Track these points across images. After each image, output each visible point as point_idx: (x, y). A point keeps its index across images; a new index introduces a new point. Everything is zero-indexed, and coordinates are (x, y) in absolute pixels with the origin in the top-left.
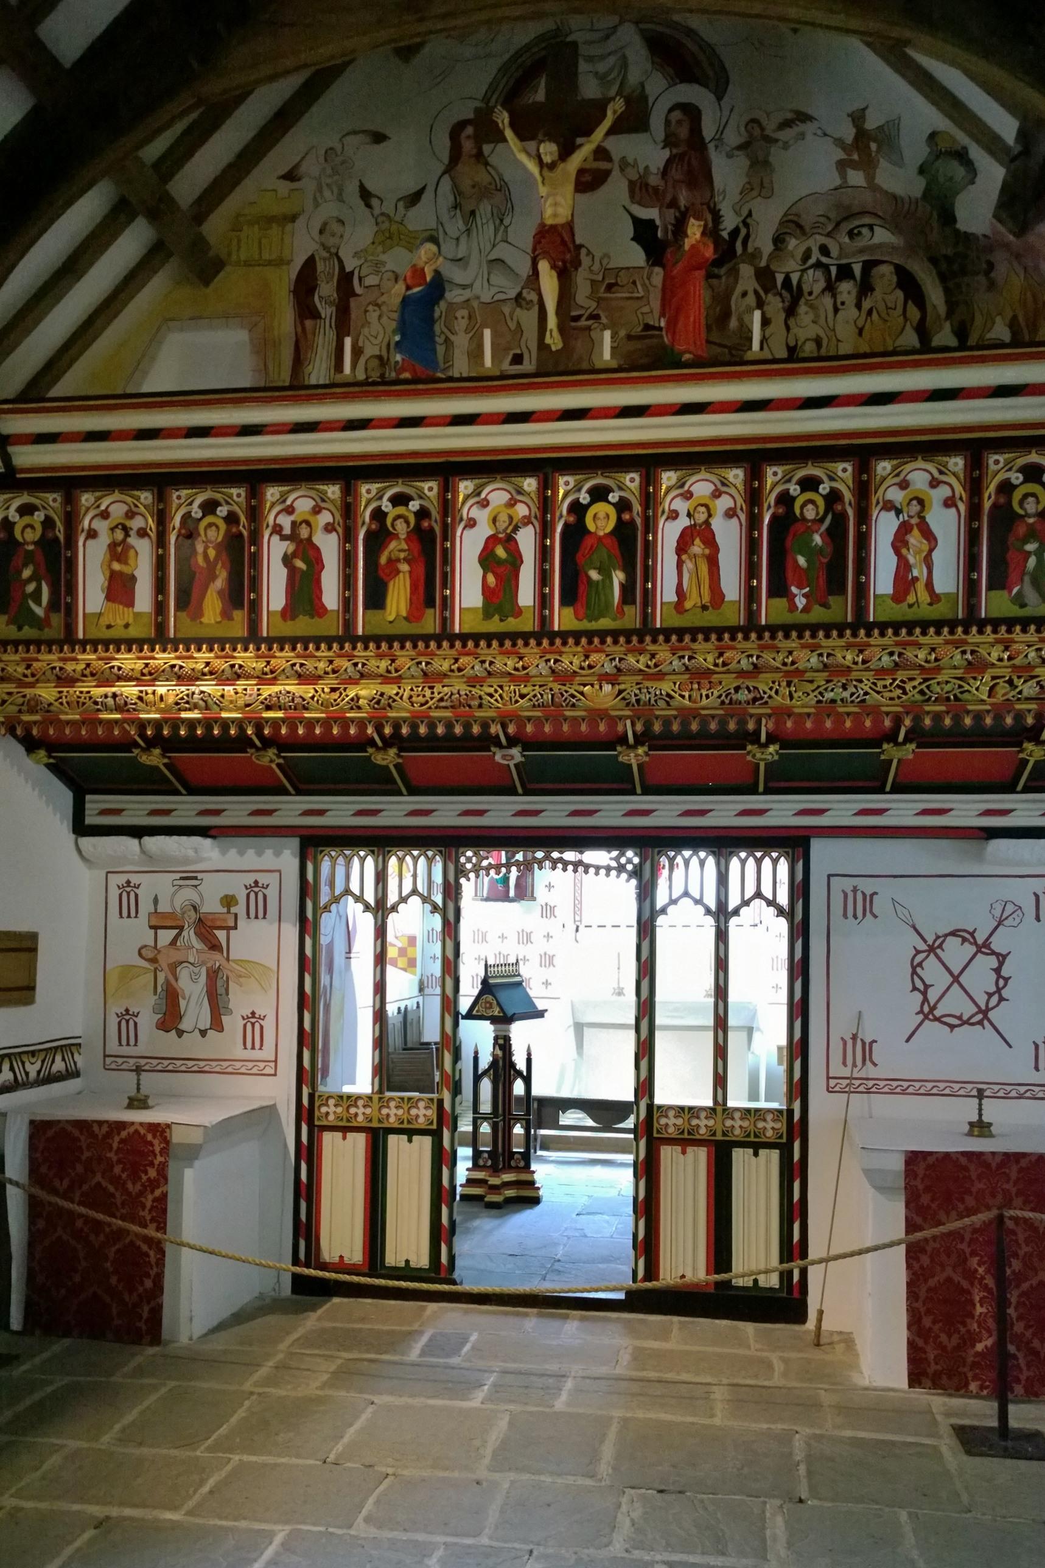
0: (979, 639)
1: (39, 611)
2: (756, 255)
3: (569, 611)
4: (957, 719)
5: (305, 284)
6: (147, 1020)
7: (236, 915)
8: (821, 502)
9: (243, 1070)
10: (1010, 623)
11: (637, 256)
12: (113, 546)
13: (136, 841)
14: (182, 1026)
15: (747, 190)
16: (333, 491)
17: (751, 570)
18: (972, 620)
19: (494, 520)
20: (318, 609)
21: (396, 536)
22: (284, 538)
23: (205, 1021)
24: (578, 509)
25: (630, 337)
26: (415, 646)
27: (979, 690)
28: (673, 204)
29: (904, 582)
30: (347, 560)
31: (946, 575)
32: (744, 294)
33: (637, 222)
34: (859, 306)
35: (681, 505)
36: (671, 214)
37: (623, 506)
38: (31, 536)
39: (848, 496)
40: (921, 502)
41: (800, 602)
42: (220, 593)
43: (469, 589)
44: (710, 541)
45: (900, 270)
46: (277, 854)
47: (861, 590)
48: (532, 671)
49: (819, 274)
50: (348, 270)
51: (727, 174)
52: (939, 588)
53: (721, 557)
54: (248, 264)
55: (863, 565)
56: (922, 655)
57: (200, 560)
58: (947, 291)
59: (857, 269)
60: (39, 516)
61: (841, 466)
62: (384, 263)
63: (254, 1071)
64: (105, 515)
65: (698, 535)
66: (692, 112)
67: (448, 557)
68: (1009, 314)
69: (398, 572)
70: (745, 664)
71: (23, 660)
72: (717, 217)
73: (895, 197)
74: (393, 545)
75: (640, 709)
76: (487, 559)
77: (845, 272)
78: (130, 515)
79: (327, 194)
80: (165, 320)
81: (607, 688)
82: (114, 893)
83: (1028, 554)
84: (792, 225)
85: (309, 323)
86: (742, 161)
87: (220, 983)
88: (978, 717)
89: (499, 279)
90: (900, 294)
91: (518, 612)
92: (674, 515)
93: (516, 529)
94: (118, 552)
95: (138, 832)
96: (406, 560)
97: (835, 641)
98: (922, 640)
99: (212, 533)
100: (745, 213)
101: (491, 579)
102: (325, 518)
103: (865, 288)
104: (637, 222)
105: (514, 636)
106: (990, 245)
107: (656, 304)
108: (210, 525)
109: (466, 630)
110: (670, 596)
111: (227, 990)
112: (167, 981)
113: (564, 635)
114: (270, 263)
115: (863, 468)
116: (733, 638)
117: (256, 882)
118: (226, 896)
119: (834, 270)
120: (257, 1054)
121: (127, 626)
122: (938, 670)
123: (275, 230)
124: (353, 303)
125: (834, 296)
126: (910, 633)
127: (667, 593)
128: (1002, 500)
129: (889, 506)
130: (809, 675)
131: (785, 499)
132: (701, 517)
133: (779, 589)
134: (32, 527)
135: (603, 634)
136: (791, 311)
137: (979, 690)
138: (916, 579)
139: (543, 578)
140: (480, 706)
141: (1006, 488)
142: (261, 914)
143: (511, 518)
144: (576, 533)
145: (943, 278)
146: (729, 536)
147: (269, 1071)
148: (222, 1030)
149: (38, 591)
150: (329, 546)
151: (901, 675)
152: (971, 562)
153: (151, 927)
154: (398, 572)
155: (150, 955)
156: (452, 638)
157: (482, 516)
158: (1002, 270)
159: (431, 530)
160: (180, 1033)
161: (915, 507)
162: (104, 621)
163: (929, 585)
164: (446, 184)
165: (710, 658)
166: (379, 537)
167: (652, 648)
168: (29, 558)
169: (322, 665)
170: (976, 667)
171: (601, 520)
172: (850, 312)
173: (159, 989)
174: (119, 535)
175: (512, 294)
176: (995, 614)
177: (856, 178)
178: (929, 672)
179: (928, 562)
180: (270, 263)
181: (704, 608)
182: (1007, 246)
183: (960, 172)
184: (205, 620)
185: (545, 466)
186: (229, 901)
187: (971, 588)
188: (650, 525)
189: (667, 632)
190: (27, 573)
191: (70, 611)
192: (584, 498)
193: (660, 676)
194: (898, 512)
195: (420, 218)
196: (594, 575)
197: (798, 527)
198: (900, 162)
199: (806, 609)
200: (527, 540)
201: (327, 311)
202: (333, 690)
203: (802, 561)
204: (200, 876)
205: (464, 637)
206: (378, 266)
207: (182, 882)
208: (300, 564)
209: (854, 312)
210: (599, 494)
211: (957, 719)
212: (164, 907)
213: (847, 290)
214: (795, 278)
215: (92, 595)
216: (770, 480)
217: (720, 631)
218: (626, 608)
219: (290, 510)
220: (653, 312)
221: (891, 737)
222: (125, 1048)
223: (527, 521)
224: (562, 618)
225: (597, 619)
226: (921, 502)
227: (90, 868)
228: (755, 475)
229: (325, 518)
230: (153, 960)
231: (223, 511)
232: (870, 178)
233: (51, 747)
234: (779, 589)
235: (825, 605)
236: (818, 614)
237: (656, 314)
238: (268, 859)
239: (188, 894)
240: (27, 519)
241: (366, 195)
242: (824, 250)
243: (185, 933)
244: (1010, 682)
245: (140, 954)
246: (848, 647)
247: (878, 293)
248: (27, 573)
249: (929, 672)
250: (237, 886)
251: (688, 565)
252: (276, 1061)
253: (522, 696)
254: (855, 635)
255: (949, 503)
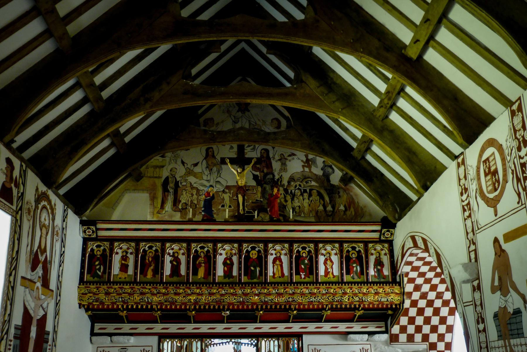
0: (345, 287)
1: (100, 274)
2: (283, 185)
3: (246, 277)
4: (341, 305)
5: (166, 182)
8: (307, 253)
10: (352, 283)
11: (254, 183)
12: (122, 257)
15: (281, 170)
16: (184, 245)
17: (291, 269)
18: (342, 282)
19: (227, 254)
20: (179, 275)
21: (201, 257)
22: (170, 256)
24: (247, 252)
25: (252, 202)
26: (206, 286)
27: (346, 299)
28: (263, 171)
29: (327, 273)
30: (188, 263)
31: (336, 272)
32: (281, 194)
33: (253, 174)
34: (309, 199)
35: (273, 252)
36: (262, 174)
37: (259, 252)
38: (99, 253)
39: (313, 252)
40: (329, 254)
41: (303, 276)
42: (152, 270)
43: (220, 271)
44: (281, 261)
45: (318, 191)
47: (317, 274)
48: (237, 293)
49: (299, 191)
50: (178, 180)
51: (276, 166)
52: (335, 274)
53: (284, 265)
54: (150, 177)
55: (317, 269)
56: (332, 290)
57: (147, 261)
58: (329, 198)
59: (308, 190)
60: (102, 248)
61: (311, 245)
62: (187, 180)
64: (121, 248)
65: (277, 259)
66: (267, 151)
67: (215, 263)
68: (344, 204)
69: (201, 266)
70: (291, 292)
71: (96, 287)
72: (274, 176)
73: (316, 175)
74: (200, 259)
75: (266, 303)
76: (225, 263)
77: (305, 191)
78: (128, 249)
79: (172, 161)
80: (126, 190)
81: (257, 297)
83: (354, 267)
84: (292, 179)
85: (166, 193)
86: (279, 163)
88: (346, 305)
89: (218, 186)
90: (318, 197)
91: (233, 277)
92: (272, 254)
93: (232, 256)
94: (124, 258)
95: (110, 335)
96: (203, 263)
97: (312, 287)
98: (332, 287)
99: (151, 254)
100: (280, 175)
101: (226, 268)
102: (182, 251)
103: (310, 195)
104: (253, 174)
105: (232, 283)
106: (338, 188)
107: (259, 195)
108: (150, 252)
109: (219, 281)
110: (272, 274)
113: (245, 283)
114: (156, 177)
115: (316, 246)
116: (288, 285)
119: (302, 190)
121: (125, 278)
122: (336, 294)
123: (158, 169)
124: (179, 189)
125: (303, 196)
126: (329, 285)
127: (270, 273)
128: (348, 254)
129: (322, 254)
130: (306, 295)
131: (298, 252)
132: (278, 255)
133: (298, 273)
134: (100, 251)
135: (255, 283)
136: (293, 199)
137: (346, 299)
138: (329, 272)
139: (240, 269)
140: (223, 302)
141: (348, 251)
143: (231, 253)
144: (247, 257)
145: (328, 194)
146: (285, 259)
149: (100, 268)
150: (183, 259)
151: (328, 295)
152: (342, 269)
154: (201, 266)
156: (217, 284)
157: (223, 252)
158: (341, 193)
159: (210, 256)
161: (328, 255)
162: (119, 277)
163: (333, 273)
164: (205, 162)
165: (282, 291)
166: (197, 256)
167: (268, 287)
168: (98, 259)
169: (181, 291)
170: (345, 293)
171: (254, 255)
172: (307, 201)
174: (124, 254)
175: (222, 190)
176: (348, 281)
177: (307, 169)
178: (334, 295)
179: (332, 268)
180: (156, 177)
181: (280, 277)
182: (342, 188)
183: (330, 170)
184: (148, 277)
185: (240, 241)
187: (342, 274)
188: (266, 257)
189: (271, 283)
190: (97, 263)
191: (110, 274)
192: (249, 249)
193: (270, 294)
194: (325, 256)
195: (197, 169)
196: (252, 268)
197: (301, 258)
198: (317, 167)
199: (304, 278)
200: (235, 259)
201: (171, 191)
202: (184, 297)
203: (303, 266)
205: (219, 283)
206: (186, 181)
208: (175, 263)
209: (308, 201)
210: (253, 248)
211: (341, 305)
213: (306, 195)
214: (293, 191)
215: (116, 269)
216: (295, 247)
217: (284, 283)
218: (261, 277)
219: (173, 249)
220: (258, 196)
221: (325, 309)
223: (235, 254)
224: (244, 279)
225: (253, 279)
226: (329, 254)
228: (291, 246)
229: (182, 251)
231: (154, 249)
232: (310, 170)
233: (93, 310)
234: (298, 273)
235: (309, 277)
236: (307, 280)
237: (259, 197)
240: (98, 249)
241: (183, 163)
242: (300, 185)
244: (352, 297)
246: (315, 288)
247: (313, 196)
248: (97, 263)
249: (334, 295)
251: (276, 267)
253: (235, 299)
254: (316, 285)
255: (336, 254)
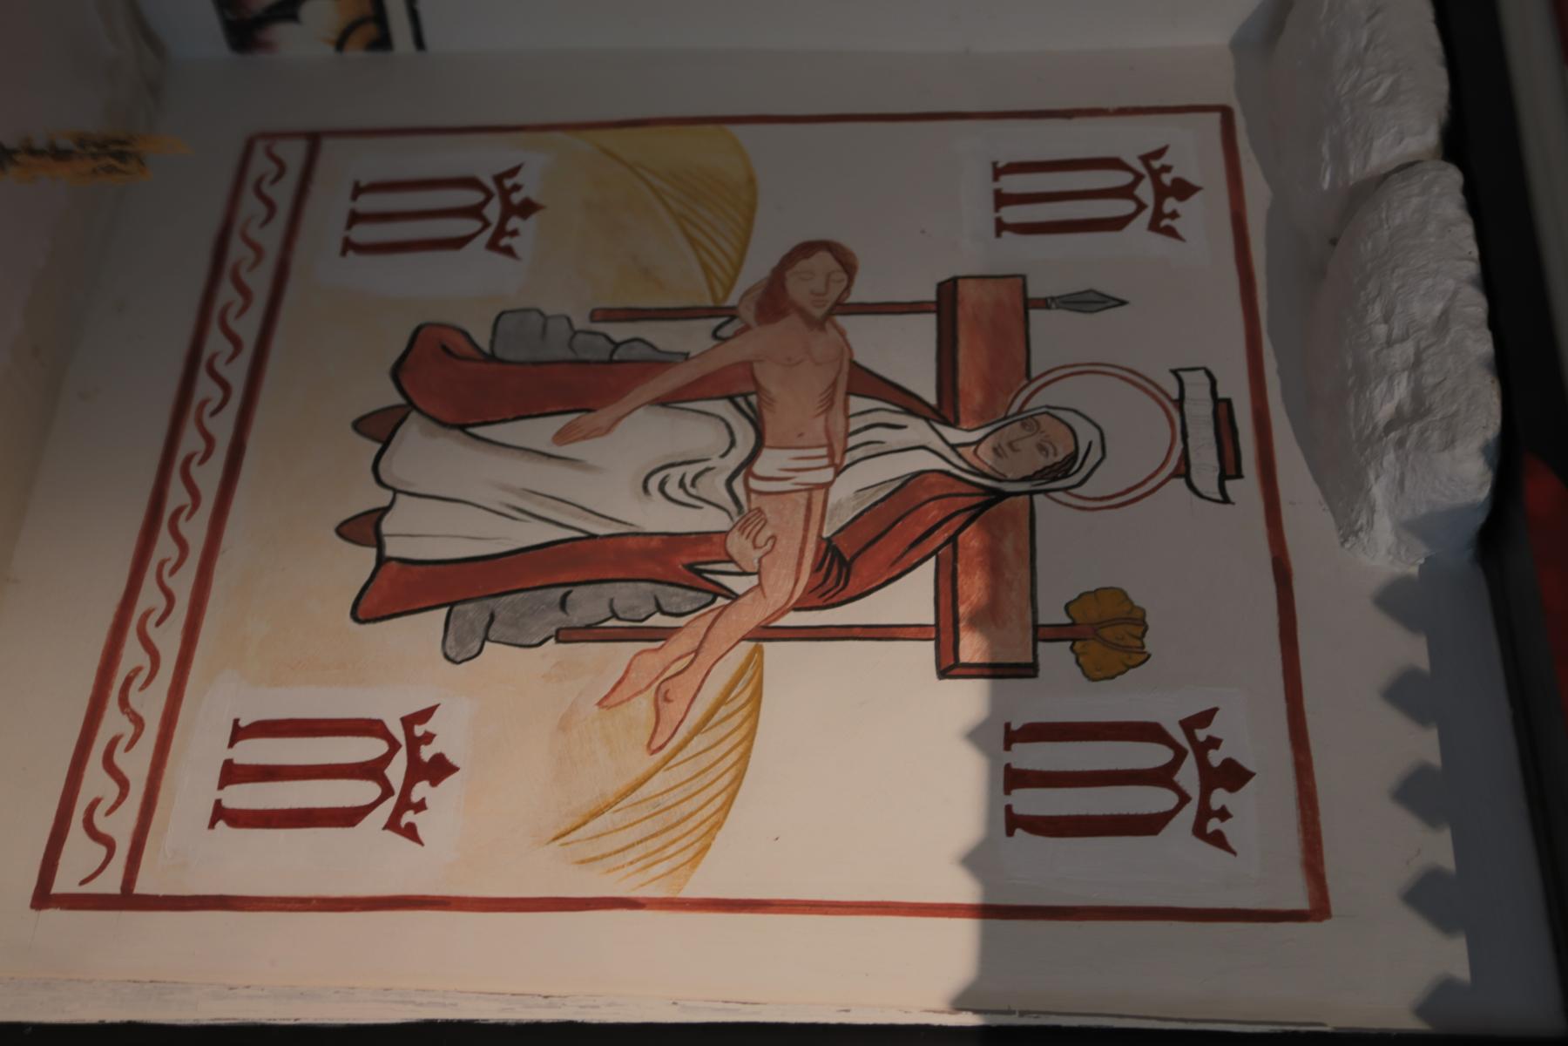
6: (467, 288)
7: (1028, 670)
9: (113, 722)
13: (1424, 136)
14: (413, 432)
23: (421, 534)
46: (1429, 897)
63: (96, 782)
82: (1128, 140)
87: (630, 597)
111: (591, 633)
112: (660, 362)
117: (1234, 776)
118: (1137, 621)
120: (193, 782)
142: (1030, 802)
147: (79, 855)
148: (365, 611)
153: (948, 291)
155: (798, 288)
160: (379, 429)
173: (619, 332)
186: (1109, 632)
204: (1246, 489)
207: (1200, 410)
212: (1053, 338)
222: (343, 204)
227: (1238, 45)
230: (773, 301)
238: (1386, 847)
239: (1135, 439)
243: (918, 430)
245: (807, 249)
250: (1212, 666)
252: (128, 900)
